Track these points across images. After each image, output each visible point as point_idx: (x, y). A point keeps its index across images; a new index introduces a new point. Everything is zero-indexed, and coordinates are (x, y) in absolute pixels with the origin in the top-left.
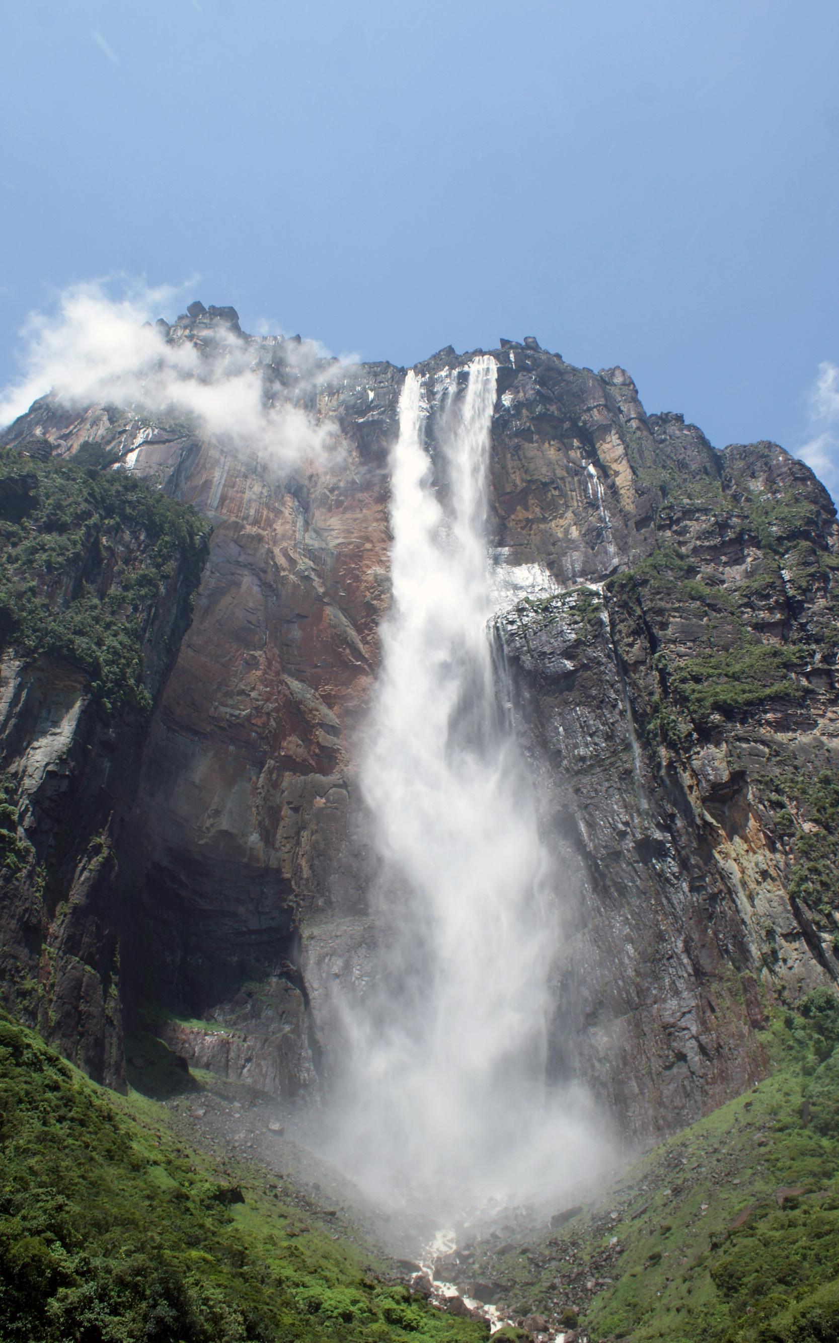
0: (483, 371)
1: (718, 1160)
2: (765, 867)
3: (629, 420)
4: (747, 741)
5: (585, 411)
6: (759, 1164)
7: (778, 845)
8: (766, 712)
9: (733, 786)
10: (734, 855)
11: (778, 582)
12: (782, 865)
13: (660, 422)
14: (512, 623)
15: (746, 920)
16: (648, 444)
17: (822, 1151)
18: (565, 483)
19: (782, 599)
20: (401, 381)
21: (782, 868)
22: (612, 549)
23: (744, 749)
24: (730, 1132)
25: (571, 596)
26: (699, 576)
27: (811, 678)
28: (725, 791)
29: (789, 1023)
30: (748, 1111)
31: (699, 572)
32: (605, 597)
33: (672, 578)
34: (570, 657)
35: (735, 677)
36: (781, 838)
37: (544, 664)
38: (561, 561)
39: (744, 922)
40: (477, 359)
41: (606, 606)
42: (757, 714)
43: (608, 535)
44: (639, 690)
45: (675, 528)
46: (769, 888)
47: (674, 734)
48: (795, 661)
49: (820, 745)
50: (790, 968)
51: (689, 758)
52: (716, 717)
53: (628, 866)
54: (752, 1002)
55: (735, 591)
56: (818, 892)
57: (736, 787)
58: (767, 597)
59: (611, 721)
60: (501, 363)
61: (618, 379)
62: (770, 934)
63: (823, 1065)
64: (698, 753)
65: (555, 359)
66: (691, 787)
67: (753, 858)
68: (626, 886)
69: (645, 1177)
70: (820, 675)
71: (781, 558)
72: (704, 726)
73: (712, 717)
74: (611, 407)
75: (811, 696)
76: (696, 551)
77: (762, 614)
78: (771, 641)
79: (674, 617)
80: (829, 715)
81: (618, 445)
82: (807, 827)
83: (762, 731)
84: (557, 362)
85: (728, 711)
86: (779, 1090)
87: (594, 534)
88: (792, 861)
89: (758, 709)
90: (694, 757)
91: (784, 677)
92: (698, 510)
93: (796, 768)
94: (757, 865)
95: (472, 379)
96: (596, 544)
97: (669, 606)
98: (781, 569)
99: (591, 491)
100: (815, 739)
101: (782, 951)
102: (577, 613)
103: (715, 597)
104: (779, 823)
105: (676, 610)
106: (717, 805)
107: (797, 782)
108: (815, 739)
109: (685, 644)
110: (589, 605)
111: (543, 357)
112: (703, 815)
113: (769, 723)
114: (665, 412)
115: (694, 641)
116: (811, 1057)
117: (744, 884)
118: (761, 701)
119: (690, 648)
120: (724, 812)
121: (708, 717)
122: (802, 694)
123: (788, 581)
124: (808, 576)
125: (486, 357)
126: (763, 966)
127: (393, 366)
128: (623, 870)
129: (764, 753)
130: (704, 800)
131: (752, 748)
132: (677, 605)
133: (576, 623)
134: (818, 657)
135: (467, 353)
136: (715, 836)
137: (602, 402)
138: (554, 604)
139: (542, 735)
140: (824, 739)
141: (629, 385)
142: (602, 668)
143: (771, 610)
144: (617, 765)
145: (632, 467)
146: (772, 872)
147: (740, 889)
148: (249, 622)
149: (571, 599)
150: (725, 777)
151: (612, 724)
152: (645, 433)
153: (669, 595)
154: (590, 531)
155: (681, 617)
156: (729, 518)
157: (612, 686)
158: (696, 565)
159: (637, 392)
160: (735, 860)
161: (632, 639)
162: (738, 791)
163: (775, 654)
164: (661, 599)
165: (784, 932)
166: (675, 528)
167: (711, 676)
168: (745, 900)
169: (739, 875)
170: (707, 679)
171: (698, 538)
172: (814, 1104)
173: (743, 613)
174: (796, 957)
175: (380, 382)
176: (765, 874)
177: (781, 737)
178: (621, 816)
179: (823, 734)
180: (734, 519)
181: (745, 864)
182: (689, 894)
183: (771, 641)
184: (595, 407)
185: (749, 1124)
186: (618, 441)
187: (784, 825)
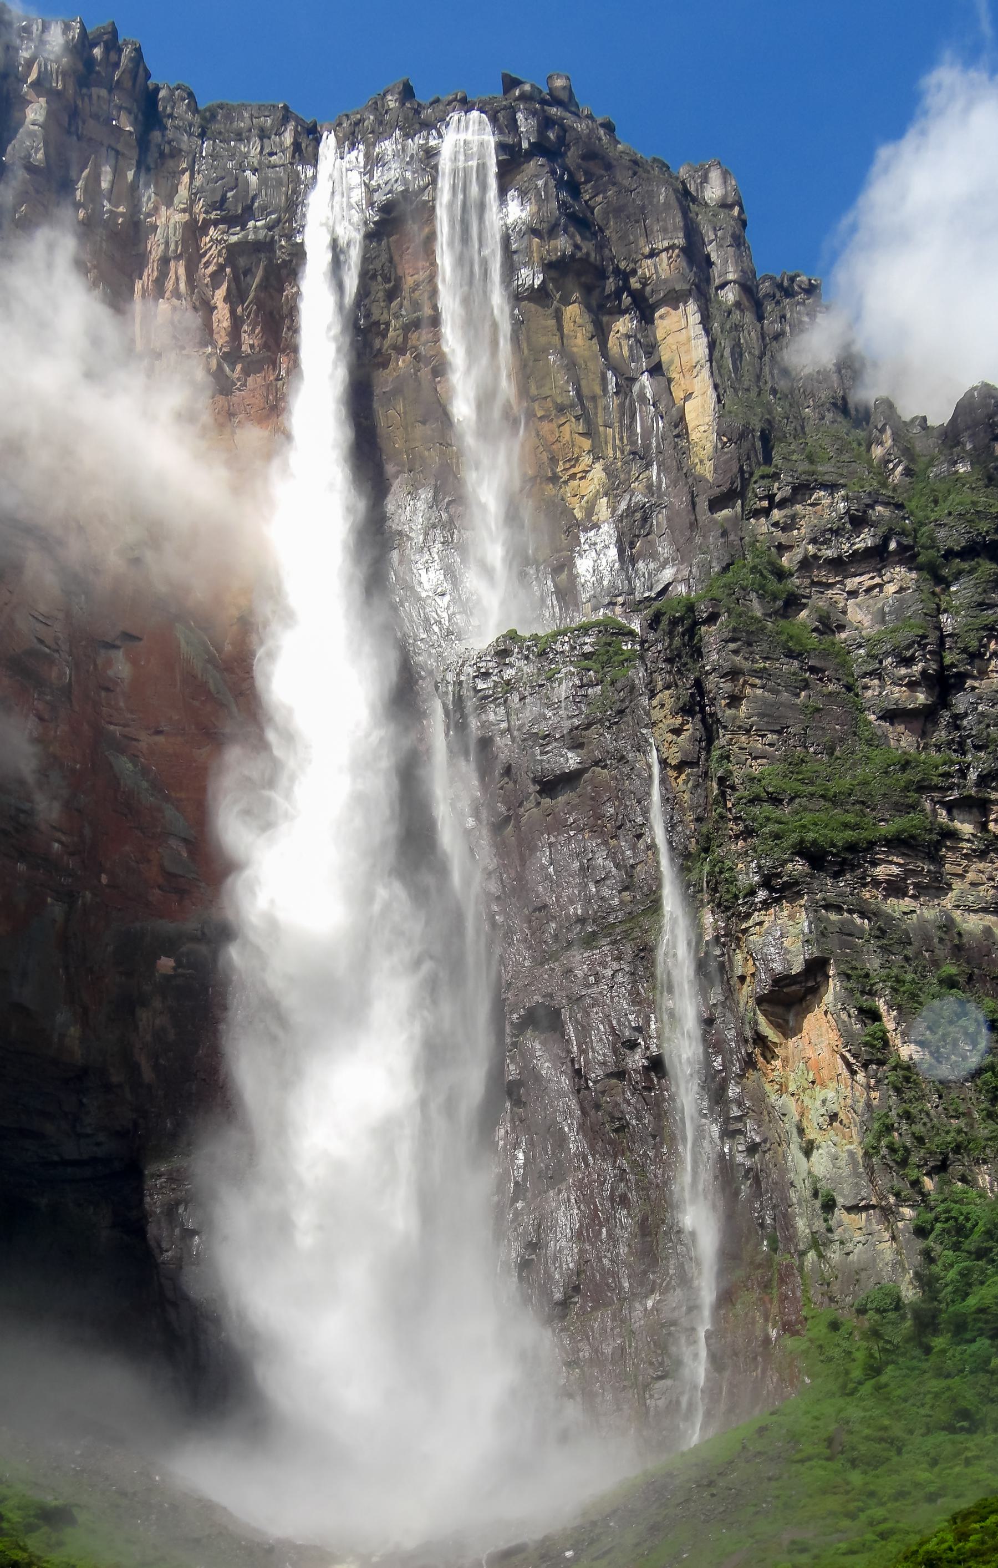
0: (466, 140)
1: (713, 1495)
2: (835, 1108)
3: (722, 286)
4: (839, 909)
5: (647, 257)
6: (766, 1502)
7: (861, 1077)
9: (806, 981)
10: (792, 1088)
11: (933, 637)
12: (861, 1106)
13: (778, 294)
14: (486, 675)
15: (796, 1183)
16: (750, 337)
17: (849, 1488)
18: (596, 407)
19: (933, 667)
20: (314, 160)
21: (860, 1112)
22: (664, 550)
23: (833, 923)
24: (733, 1462)
25: (586, 634)
26: (804, 614)
28: (794, 988)
29: (835, 1326)
30: (761, 1436)
31: (805, 606)
32: (642, 643)
33: (759, 614)
34: (577, 746)
35: (834, 800)
37: (534, 755)
38: (573, 565)
40: (455, 116)
41: (642, 658)
42: (860, 866)
43: (660, 519)
44: (683, 810)
45: (776, 514)
46: (835, 1139)
47: (728, 891)
48: (936, 780)
50: (848, 1254)
53: (633, 1094)
54: (787, 1298)
55: (860, 646)
56: (906, 1149)
57: (810, 984)
59: (631, 861)
60: (501, 132)
61: (714, 191)
62: (829, 1206)
63: (872, 1382)
64: (761, 924)
65: (602, 132)
66: (742, 979)
67: (820, 1094)
68: (628, 1123)
69: (615, 1512)
70: (970, 807)
71: (944, 590)
74: (694, 253)
78: (903, 740)
80: (971, 876)
81: (696, 337)
83: (866, 895)
84: (605, 139)
85: (816, 857)
86: (807, 1413)
87: (638, 515)
88: (875, 1102)
89: (864, 858)
91: (913, 807)
94: (824, 1101)
95: (445, 163)
96: (638, 536)
98: (939, 611)
99: (639, 430)
101: (840, 1230)
102: (596, 666)
103: (825, 654)
104: (866, 1044)
106: (779, 1010)
107: (904, 982)
109: (763, 736)
110: (616, 654)
111: (581, 127)
112: (756, 1023)
114: (792, 273)
115: (779, 732)
116: (857, 1373)
118: (872, 844)
119: (771, 745)
120: (787, 1022)
121: (786, 862)
122: (935, 837)
123: (949, 635)
124: (982, 629)
125: (475, 114)
126: (810, 1248)
127: (299, 121)
128: (628, 1102)
129: (862, 930)
130: (760, 1001)
131: (842, 923)
133: (591, 685)
134: (973, 776)
135: (437, 101)
136: (769, 1056)
137: (680, 241)
138: (558, 647)
139: (520, 878)
140: (957, 915)
141: (731, 207)
142: (626, 770)
144: (634, 935)
148: (41, 641)
149: (587, 640)
151: (632, 866)
152: (749, 318)
153: (750, 645)
154: (629, 512)
156: (872, 507)
157: (639, 802)
158: (801, 591)
159: (744, 224)
161: (679, 720)
163: (905, 765)
164: (736, 652)
165: (848, 1204)
167: (797, 796)
168: (800, 1156)
170: (792, 800)
172: (850, 1432)
173: (866, 688)
174: (858, 1239)
175: (271, 154)
176: (834, 1117)
178: (631, 1017)
179: (958, 907)
180: (879, 508)
181: (807, 1101)
182: (718, 1142)
183: (903, 744)
185: (759, 1453)
186: (699, 329)
187: (873, 1046)
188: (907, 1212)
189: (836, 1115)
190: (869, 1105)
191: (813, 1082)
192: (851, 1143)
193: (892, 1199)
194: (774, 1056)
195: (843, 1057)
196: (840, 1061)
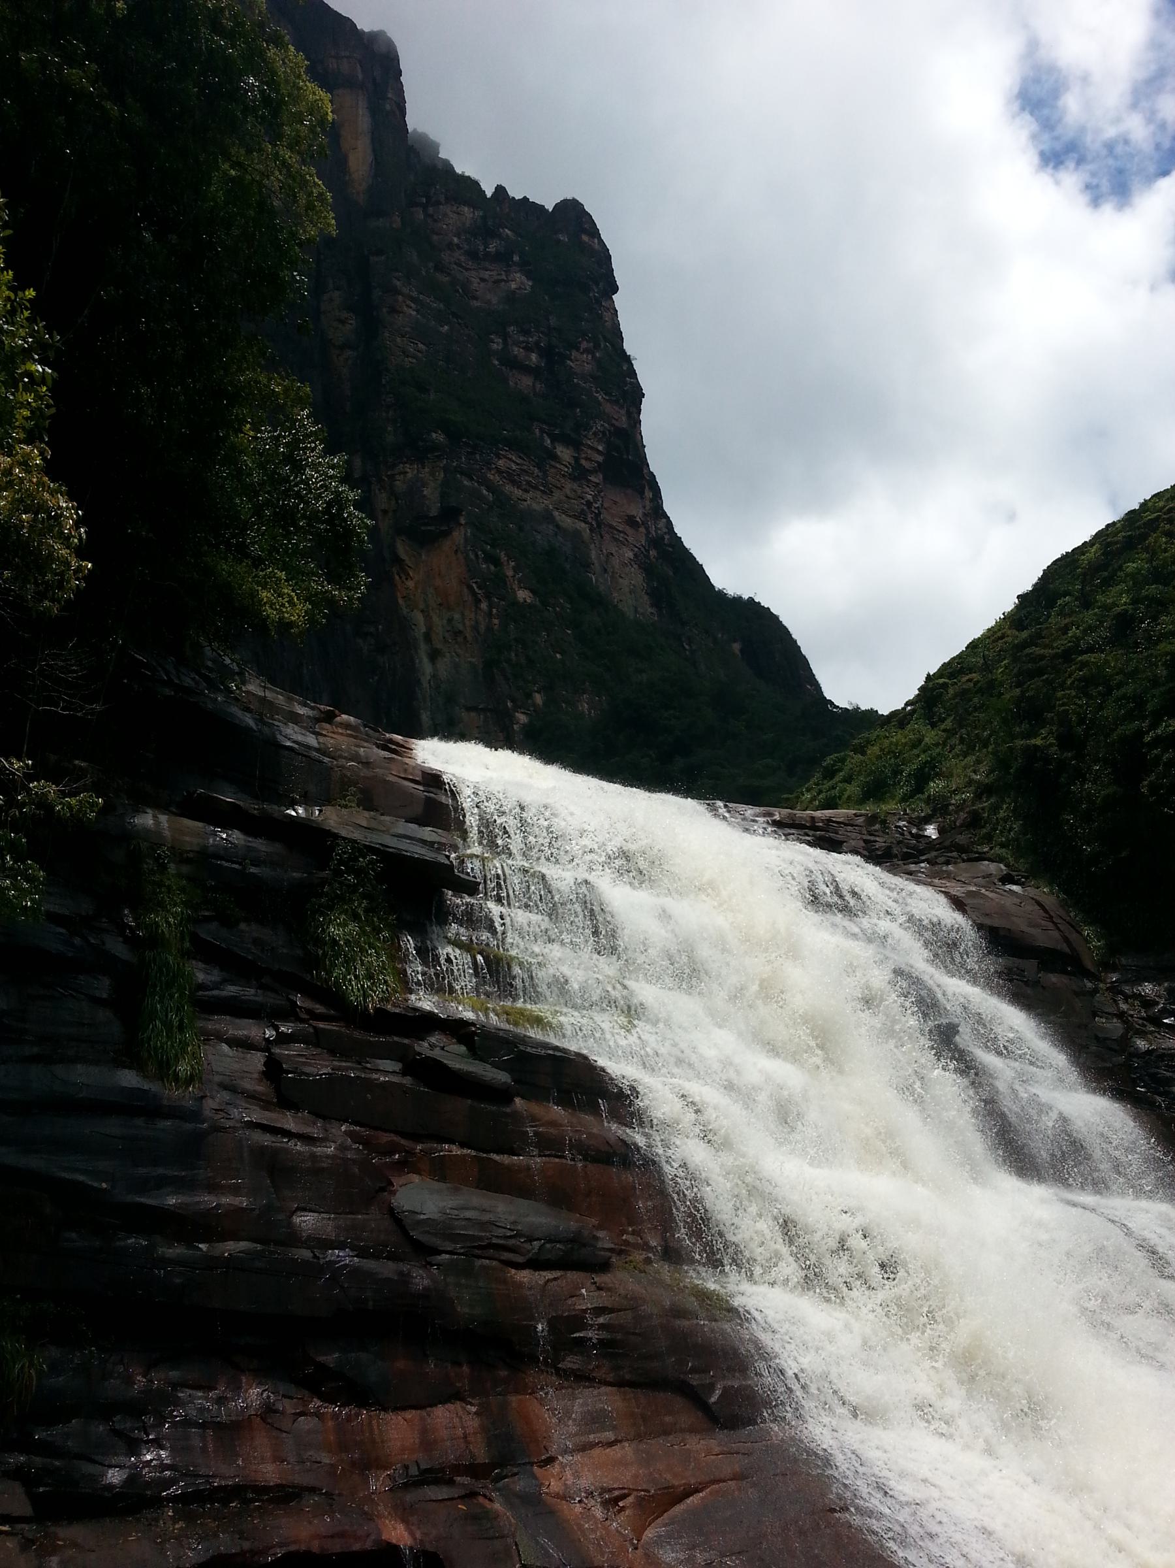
2: (461, 627)
8: (498, 457)
12: (482, 628)
27: (556, 444)
36: (488, 597)
39: (419, 682)
49: (548, 517)
51: (392, 478)
52: (438, 437)
57: (443, 528)
58: (526, 333)
66: (385, 512)
72: (421, 444)
73: (434, 435)
75: (553, 463)
76: (450, 246)
77: (516, 350)
79: (408, 306)
82: (523, 595)
90: (397, 477)
92: (466, 203)
93: (521, 529)
94: (450, 620)
97: (405, 290)
100: (547, 510)
105: (413, 299)
108: (547, 510)
113: (499, 472)
117: (428, 637)
132: (415, 294)
136: (404, 578)
140: (556, 513)
143: (528, 349)
145: (374, 150)
146: (469, 634)
147: (423, 648)
150: (434, 512)
155: (417, 311)
160: (422, 611)
162: (446, 534)
166: (431, 210)
168: (426, 660)
169: (424, 630)
171: (458, 235)
177: (508, 488)
181: (435, 619)
184: (347, 57)
188: (522, 718)
189: (460, 632)
190: (489, 629)
191: (440, 605)
192: (472, 657)
193: (509, 704)
194: (408, 577)
195: (470, 588)
196: (465, 590)
